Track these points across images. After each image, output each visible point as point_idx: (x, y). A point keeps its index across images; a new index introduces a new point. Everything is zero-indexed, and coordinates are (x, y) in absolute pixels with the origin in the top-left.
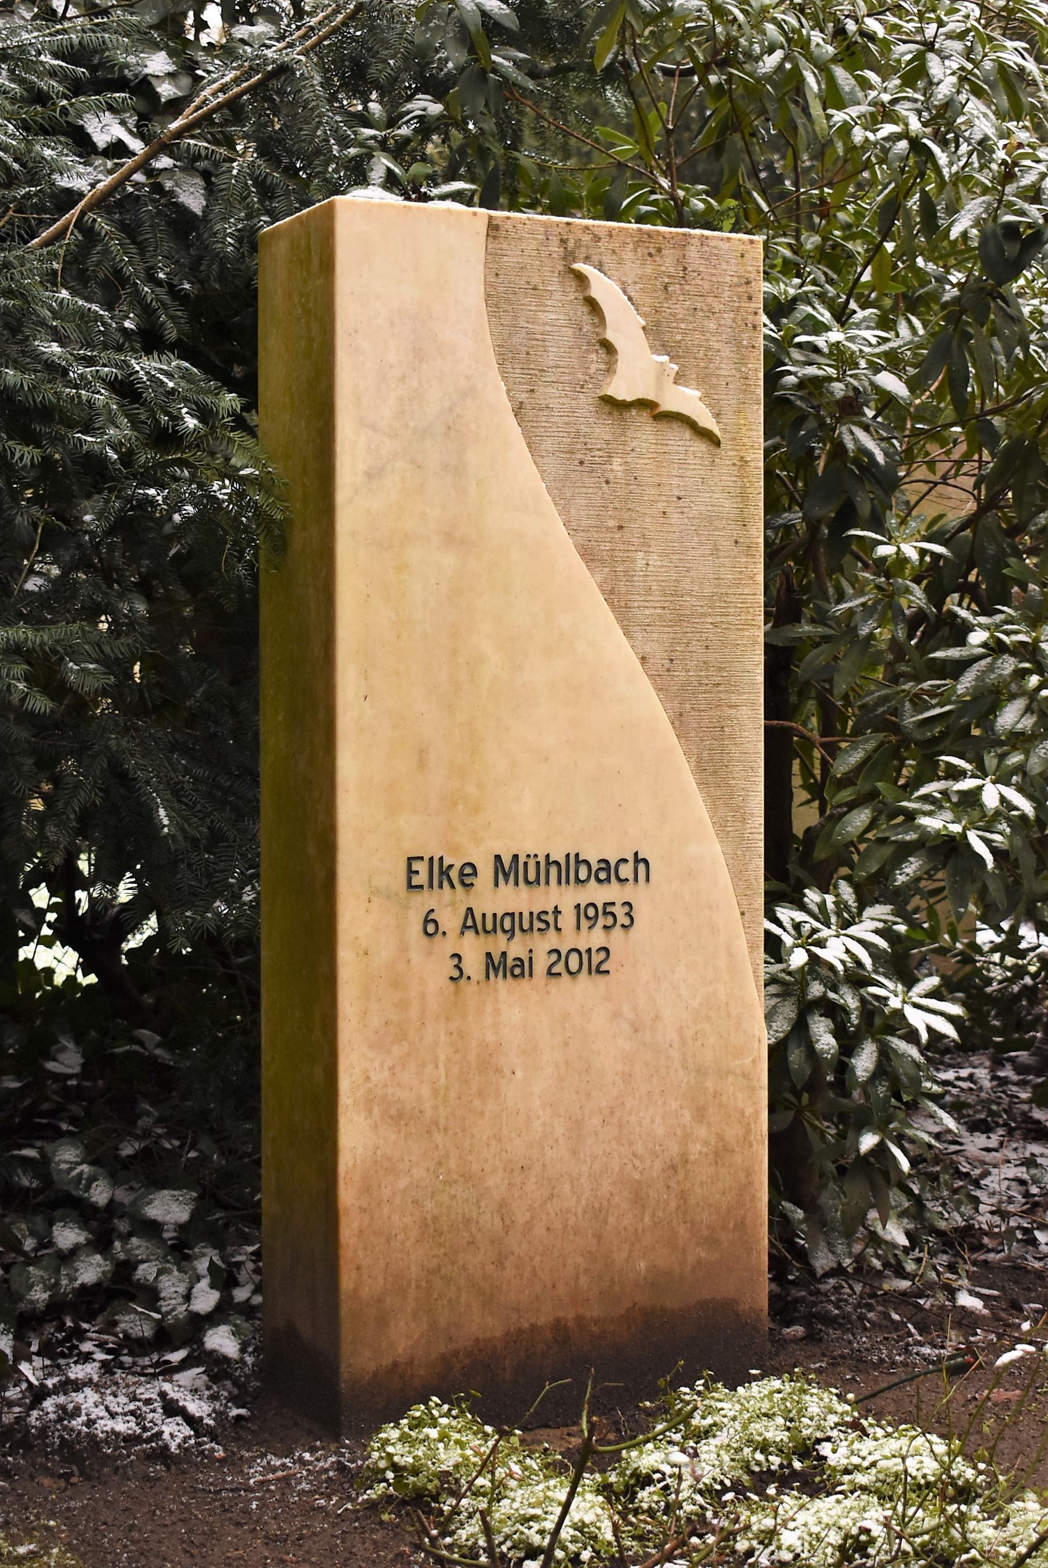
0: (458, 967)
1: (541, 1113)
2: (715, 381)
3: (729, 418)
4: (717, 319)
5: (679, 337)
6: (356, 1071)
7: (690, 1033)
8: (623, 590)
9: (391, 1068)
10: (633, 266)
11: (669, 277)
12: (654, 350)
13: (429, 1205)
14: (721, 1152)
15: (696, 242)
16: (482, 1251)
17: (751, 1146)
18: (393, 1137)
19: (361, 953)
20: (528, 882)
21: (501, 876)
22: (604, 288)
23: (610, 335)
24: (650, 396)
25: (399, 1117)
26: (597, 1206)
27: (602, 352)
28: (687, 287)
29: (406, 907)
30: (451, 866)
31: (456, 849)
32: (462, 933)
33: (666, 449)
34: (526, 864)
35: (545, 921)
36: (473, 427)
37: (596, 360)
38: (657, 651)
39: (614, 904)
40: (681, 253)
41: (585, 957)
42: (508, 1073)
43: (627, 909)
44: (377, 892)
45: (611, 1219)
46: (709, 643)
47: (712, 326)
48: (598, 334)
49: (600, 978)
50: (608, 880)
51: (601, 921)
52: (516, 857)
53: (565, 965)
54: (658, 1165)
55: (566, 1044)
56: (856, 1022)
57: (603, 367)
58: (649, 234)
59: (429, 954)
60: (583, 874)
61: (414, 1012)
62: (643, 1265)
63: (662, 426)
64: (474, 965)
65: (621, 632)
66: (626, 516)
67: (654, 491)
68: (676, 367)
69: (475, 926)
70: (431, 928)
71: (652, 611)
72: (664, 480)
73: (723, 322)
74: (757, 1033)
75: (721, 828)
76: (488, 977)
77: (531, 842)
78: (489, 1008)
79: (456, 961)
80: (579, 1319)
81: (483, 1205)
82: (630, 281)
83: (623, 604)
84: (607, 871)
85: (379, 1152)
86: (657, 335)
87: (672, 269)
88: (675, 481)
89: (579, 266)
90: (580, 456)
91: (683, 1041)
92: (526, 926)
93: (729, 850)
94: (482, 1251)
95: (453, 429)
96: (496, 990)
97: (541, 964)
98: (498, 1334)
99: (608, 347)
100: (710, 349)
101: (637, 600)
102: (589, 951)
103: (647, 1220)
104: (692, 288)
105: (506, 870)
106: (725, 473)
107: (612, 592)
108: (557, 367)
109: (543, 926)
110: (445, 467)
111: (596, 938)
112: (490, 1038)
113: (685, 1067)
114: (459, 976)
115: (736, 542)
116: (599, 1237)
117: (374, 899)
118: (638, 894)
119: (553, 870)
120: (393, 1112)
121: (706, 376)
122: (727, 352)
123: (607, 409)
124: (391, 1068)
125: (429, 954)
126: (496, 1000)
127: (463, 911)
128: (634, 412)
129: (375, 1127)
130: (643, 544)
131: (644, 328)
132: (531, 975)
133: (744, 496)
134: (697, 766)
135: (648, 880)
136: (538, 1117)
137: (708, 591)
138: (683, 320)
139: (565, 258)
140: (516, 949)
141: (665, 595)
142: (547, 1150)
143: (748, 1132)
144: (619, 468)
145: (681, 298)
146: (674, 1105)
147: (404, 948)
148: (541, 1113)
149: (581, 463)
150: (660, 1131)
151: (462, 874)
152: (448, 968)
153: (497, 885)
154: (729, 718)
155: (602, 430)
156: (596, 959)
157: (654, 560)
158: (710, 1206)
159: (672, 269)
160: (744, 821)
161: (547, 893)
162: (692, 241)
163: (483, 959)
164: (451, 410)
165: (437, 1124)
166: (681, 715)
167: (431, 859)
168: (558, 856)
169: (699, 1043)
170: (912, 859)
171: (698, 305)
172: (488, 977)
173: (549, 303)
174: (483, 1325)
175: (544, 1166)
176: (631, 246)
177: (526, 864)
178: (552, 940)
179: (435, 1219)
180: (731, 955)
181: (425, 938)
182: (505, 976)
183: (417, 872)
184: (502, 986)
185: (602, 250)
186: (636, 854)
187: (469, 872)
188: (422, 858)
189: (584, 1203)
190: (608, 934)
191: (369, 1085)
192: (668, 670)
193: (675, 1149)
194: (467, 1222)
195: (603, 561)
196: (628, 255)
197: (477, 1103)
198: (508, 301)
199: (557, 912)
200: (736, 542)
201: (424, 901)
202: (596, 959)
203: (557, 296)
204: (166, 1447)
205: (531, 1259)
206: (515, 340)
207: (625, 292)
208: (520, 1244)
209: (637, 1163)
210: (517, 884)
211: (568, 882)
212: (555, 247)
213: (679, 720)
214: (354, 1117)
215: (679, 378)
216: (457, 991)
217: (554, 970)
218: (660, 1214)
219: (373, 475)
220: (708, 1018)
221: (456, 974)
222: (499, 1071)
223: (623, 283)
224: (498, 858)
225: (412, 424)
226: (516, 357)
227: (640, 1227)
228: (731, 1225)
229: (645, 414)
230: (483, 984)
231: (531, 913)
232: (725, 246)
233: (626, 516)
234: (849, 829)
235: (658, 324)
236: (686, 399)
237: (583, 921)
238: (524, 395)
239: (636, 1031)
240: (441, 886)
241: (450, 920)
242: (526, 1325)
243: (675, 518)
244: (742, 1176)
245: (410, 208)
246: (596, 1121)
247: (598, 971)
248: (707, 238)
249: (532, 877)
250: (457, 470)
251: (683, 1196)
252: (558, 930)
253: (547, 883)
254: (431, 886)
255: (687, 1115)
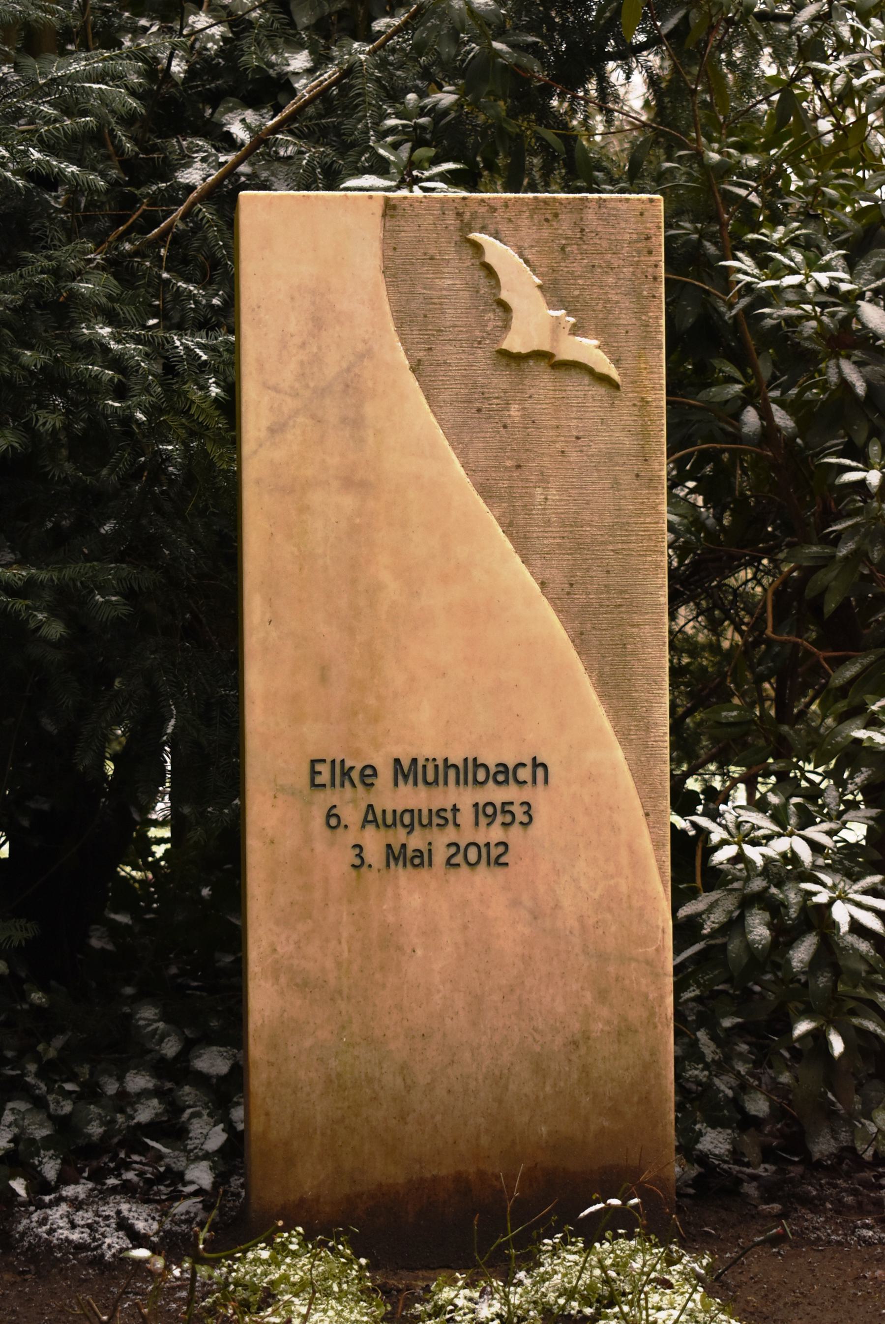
0: (359, 855)
1: (441, 987)
2: (614, 330)
3: (629, 363)
4: (616, 274)
5: (577, 293)
6: (264, 943)
7: (591, 922)
8: (522, 522)
9: (297, 943)
10: (528, 231)
11: (566, 238)
12: (552, 306)
13: (333, 1063)
14: (624, 1032)
15: (593, 205)
16: (385, 1106)
17: (656, 1027)
18: (299, 1002)
19: (268, 841)
20: (426, 783)
21: (400, 777)
22: (497, 252)
23: (504, 295)
24: (546, 347)
25: (304, 984)
26: (497, 1072)
27: (499, 312)
28: (585, 247)
29: (310, 803)
30: (352, 768)
31: (357, 753)
32: (363, 826)
33: (564, 394)
34: (424, 767)
35: (445, 818)
36: (370, 384)
37: (492, 318)
38: (556, 576)
39: (512, 803)
40: (578, 217)
41: (484, 851)
42: (409, 951)
43: (525, 808)
44: (282, 789)
45: (512, 1087)
46: (609, 568)
47: (611, 280)
48: (495, 295)
49: (499, 871)
50: (506, 781)
51: (500, 819)
52: (414, 761)
53: (459, 857)
54: (559, 1040)
55: (465, 927)
56: (794, 916)
57: (500, 324)
58: (545, 201)
59: (332, 844)
60: (481, 776)
61: (318, 895)
62: (544, 1129)
63: (561, 373)
64: (374, 852)
65: (518, 560)
66: (524, 456)
67: (552, 433)
68: (572, 320)
69: (375, 820)
70: (333, 821)
71: (551, 540)
72: (564, 423)
73: (622, 276)
74: (661, 924)
75: (624, 737)
76: (388, 865)
77: (429, 746)
78: (390, 893)
79: (357, 851)
80: (481, 1173)
81: (385, 1066)
82: (526, 245)
83: (522, 535)
84: (505, 774)
85: (285, 1014)
86: (554, 292)
87: (569, 232)
88: (574, 423)
89: (476, 236)
90: (478, 405)
91: (583, 928)
92: (425, 821)
93: (634, 757)
94: (385, 1106)
95: (351, 387)
96: (396, 878)
97: (440, 855)
98: (401, 1180)
99: (505, 307)
100: (608, 301)
101: (536, 531)
102: (488, 845)
103: (548, 1089)
104: (590, 247)
105: (406, 771)
106: (626, 414)
107: (511, 524)
108: (454, 326)
109: (442, 822)
110: (344, 420)
111: (496, 834)
112: (391, 919)
113: (585, 952)
114: (360, 864)
115: (637, 476)
116: (500, 1101)
117: (279, 795)
118: (539, 797)
119: (452, 773)
120: (299, 981)
121: (606, 326)
122: (626, 303)
123: (504, 361)
124: (297, 943)
125: (332, 844)
126: (397, 886)
127: (363, 807)
128: (531, 363)
129: (282, 993)
130: (541, 481)
131: (540, 287)
132: (430, 864)
133: (645, 434)
134: (598, 680)
135: (546, 781)
136: (439, 991)
137: (608, 521)
138: (580, 277)
139: (461, 230)
140: (416, 841)
141: (565, 526)
142: (448, 1021)
143: (652, 1014)
144: (517, 413)
145: (579, 257)
146: (575, 987)
147: (308, 839)
148: (441, 987)
149: (479, 410)
150: (561, 1009)
151: (362, 775)
152: (350, 856)
153: (396, 784)
154: (631, 636)
155: (500, 381)
156: (495, 852)
157: (553, 494)
158: (613, 1080)
159: (569, 232)
160: (647, 729)
161: (445, 793)
162: (590, 205)
163: (384, 850)
164: (348, 370)
165: (340, 993)
166: (582, 633)
167: (333, 762)
168: (456, 759)
169: (600, 931)
170: (863, 769)
171: (596, 262)
172: (388, 865)
173: (446, 270)
174: (385, 1172)
175: (445, 1035)
176: (527, 214)
177: (424, 767)
178: (450, 834)
179: (339, 1075)
180: (632, 851)
181: (328, 832)
182: (405, 865)
183: (320, 773)
184: (403, 875)
185: (499, 219)
186: (534, 759)
187: (369, 774)
188: (324, 761)
189: (484, 1070)
190: (506, 831)
191: (276, 956)
192: (568, 593)
193: (575, 1026)
194: (370, 1080)
195: (501, 498)
196: (524, 222)
197: (378, 976)
198: (406, 272)
199: (455, 809)
200: (637, 476)
201: (329, 797)
202: (495, 852)
203: (455, 263)
204: (103, 1255)
205: (433, 1117)
206: (413, 305)
207: (521, 256)
208: (421, 1103)
209: (538, 1037)
210: (415, 784)
211: (466, 783)
212: (451, 221)
213: (580, 640)
214: (262, 983)
215: (575, 330)
216: (359, 877)
217: (453, 861)
218: (562, 1084)
219: (275, 430)
220: (610, 910)
221: (358, 862)
222: (399, 948)
223: (519, 247)
224: (397, 761)
225: (312, 385)
226: (415, 321)
227: (541, 1094)
228: (636, 1099)
229: (543, 364)
230: (384, 871)
231: (430, 811)
232: (624, 206)
233: (524, 456)
234: (839, 739)
235: (555, 282)
236: (587, 349)
237: (481, 818)
238: (422, 354)
239: (535, 918)
240: (343, 785)
241: (351, 815)
242: (428, 1175)
243: (574, 456)
244: (647, 1056)
245: (308, 197)
246: (496, 997)
247: (497, 863)
248: (605, 200)
249: (430, 777)
250: (355, 423)
251: (585, 1070)
252: (457, 825)
253: (446, 783)
254: (333, 784)
255: (588, 997)
